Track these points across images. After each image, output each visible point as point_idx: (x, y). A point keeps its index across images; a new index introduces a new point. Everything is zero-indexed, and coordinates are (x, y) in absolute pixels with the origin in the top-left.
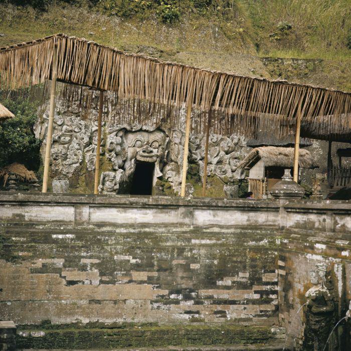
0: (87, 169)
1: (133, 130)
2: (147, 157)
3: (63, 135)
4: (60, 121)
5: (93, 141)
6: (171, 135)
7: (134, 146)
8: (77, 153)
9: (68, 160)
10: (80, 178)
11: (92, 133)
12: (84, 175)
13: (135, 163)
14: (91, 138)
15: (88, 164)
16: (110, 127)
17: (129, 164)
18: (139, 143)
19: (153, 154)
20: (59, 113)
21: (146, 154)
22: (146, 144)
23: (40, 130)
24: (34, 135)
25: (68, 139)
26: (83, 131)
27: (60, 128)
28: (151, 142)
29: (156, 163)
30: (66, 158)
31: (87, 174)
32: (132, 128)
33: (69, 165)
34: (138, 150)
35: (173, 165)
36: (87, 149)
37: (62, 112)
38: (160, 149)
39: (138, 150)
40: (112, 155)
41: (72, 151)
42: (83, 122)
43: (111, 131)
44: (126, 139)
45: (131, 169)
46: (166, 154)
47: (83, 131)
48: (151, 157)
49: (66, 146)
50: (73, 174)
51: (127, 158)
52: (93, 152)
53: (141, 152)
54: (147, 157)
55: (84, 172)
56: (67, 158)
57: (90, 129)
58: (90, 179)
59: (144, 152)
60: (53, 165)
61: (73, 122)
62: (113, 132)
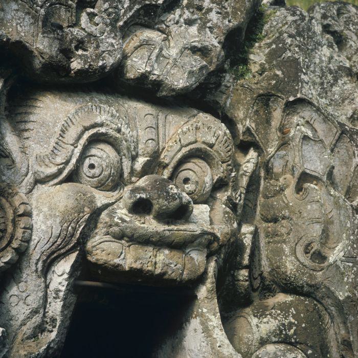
1: (76, 65)
2: (160, 243)
6: (274, 137)
7: (73, 177)
13: (74, 288)
17: (34, 300)
18: (103, 154)
19: (192, 228)
21: (150, 225)
22: (147, 169)
28: (170, 156)
29: (203, 292)
32: (67, 53)
34: (101, 198)
35: (284, 307)
38: (221, 207)
39: (101, 198)
44: (19, 132)
45: (40, 329)
46: (248, 241)
48: (180, 246)
51: (22, 253)
53: (122, 212)
54: (160, 243)
59: (140, 207)
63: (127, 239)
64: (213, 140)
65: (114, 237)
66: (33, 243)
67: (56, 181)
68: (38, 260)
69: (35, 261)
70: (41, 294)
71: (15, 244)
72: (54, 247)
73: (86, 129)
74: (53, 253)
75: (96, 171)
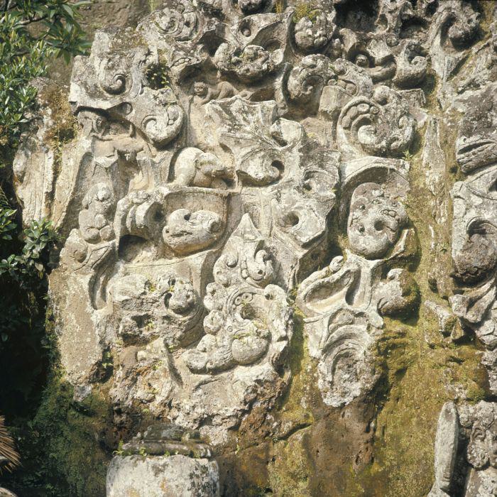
0: (316, 399)
3: (177, 197)
4: (162, 118)
5: (352, 233)
8: (259, 301)
9: (207, 340)
10: (275, 450)
11: (343, 191)
12: (299, 436)
14: (337, 220)
15: (323, 367)
16: (468, 132)
20: (156, 76)
23: (50, 177)
24: (18, 206)
25: (205, 217)
26: (294, 172)
27: (163, 157)
30: (192, 336)
31: (317, 430)
33: (216, 371)
36: (316, 277)
37: (177, 70)
40: (483, 304)
41: (231, 291)
42: (290, 130)
43: (471, 159)
47: (294, 172)
49: (197, 260)
50: (234, 429)
52: (349, 298)
55: (298, 415)
56: (201, 333)
57: (332, 166)
58: (337, 462)
60: (120, 373)
61: (235, 126)
62: (481, 166)
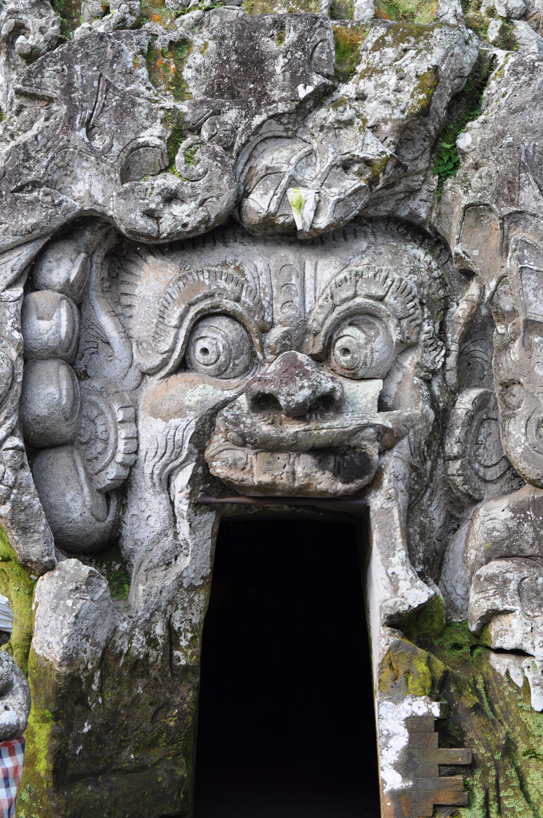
63: (250, 446)
64: (381, 293)
65: (234, 444)
66: (142, 454)
67: (163, 373)
68: (152, 473)
69: (149, 476)
70: (165, 514)
71: (119, 458)
72: (164, 459)
73: (191, 305)
74: (166, 465)
75: (212, 357)
